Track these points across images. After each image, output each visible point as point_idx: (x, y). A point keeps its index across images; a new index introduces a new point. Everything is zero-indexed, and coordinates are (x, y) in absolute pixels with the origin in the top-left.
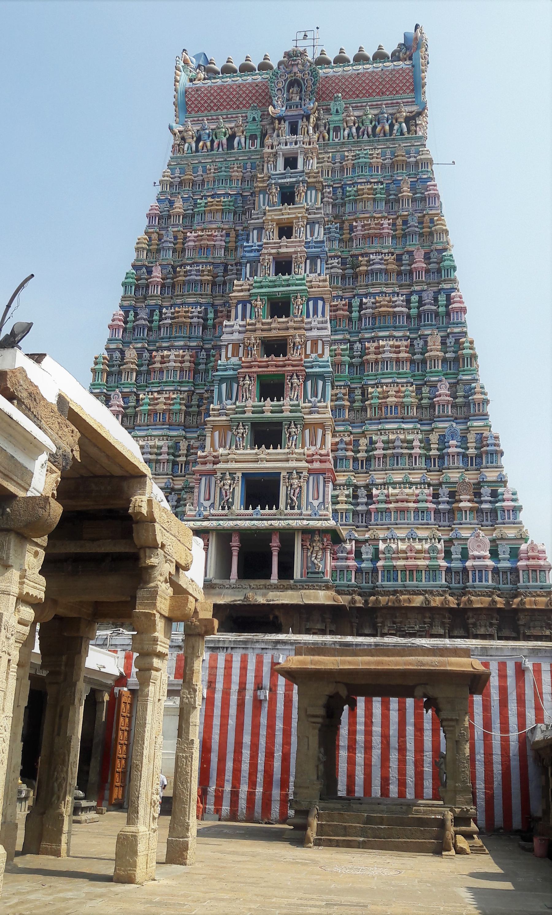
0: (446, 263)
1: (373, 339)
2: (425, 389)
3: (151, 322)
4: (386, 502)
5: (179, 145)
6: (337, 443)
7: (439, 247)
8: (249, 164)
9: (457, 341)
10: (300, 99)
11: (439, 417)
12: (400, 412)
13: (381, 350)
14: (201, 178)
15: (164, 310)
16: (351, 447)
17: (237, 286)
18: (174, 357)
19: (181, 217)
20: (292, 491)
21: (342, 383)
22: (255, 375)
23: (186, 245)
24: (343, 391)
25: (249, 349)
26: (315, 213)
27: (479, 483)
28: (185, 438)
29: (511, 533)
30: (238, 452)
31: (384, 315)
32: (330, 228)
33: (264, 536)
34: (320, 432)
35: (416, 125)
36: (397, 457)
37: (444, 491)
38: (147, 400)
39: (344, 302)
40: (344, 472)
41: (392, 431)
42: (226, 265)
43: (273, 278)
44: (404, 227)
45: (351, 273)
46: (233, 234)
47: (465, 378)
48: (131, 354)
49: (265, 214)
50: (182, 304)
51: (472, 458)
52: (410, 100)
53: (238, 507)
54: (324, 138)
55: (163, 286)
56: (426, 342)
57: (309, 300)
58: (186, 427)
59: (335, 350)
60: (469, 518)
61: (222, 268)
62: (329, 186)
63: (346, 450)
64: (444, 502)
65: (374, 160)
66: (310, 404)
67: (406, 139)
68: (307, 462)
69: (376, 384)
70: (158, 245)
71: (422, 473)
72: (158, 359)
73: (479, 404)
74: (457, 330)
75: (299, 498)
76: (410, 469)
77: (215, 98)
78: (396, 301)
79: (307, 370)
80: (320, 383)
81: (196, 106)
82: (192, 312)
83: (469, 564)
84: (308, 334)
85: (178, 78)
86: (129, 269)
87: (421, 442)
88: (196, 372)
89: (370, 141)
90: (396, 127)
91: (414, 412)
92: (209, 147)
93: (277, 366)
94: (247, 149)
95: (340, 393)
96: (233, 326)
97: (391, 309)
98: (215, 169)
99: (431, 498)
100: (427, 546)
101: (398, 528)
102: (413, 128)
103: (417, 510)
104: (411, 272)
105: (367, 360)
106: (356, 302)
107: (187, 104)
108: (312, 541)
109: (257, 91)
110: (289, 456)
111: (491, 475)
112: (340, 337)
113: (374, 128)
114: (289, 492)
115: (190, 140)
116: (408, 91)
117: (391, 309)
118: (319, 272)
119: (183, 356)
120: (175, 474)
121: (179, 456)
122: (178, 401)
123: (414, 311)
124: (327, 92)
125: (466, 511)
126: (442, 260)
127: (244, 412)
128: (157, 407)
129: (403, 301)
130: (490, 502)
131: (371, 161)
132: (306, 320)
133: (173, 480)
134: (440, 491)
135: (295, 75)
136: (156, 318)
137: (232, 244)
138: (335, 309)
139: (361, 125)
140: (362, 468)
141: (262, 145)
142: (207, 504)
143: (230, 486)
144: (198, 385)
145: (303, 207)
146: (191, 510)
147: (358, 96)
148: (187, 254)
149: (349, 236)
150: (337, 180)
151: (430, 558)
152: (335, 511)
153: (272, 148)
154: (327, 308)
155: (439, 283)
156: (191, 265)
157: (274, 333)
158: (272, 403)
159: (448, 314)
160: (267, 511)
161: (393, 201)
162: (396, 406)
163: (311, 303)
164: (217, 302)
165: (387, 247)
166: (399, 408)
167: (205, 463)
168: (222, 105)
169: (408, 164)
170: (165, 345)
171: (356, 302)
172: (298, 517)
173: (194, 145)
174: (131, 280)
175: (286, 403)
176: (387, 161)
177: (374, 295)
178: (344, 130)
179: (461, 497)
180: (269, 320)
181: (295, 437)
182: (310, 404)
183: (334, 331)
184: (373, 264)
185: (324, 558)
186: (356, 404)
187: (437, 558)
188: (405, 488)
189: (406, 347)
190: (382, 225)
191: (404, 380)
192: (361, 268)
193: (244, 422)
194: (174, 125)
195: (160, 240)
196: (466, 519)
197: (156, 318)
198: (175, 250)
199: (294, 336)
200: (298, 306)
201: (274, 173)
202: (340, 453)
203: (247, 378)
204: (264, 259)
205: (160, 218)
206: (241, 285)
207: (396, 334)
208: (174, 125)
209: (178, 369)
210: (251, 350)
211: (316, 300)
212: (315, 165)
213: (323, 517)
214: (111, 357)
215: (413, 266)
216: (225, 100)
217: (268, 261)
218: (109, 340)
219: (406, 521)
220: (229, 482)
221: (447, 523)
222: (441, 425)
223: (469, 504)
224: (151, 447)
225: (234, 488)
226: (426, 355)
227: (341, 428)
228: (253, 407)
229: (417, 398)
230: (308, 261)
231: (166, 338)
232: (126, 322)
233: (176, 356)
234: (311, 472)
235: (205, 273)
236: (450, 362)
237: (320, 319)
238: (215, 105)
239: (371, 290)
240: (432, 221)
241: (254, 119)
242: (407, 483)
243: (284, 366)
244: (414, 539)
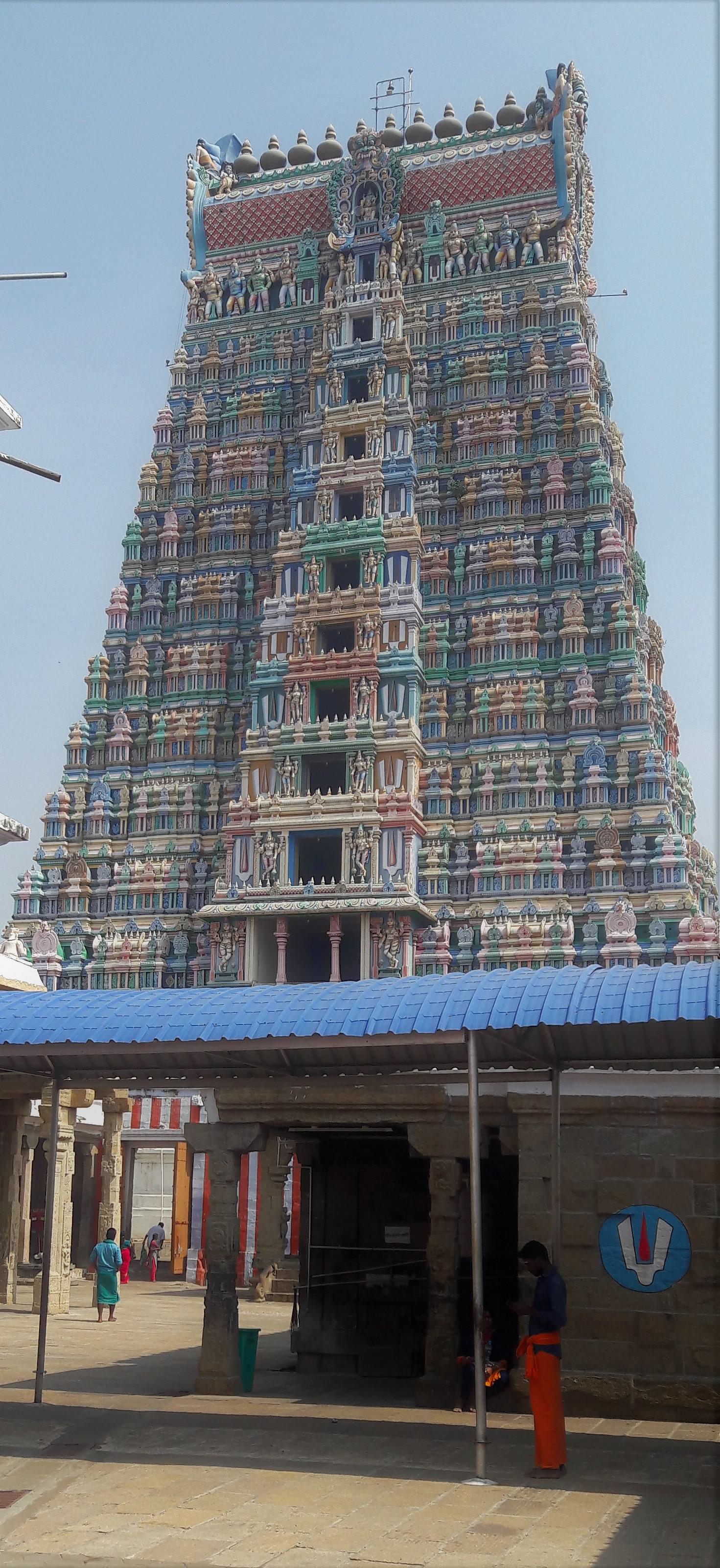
0: (595, 480)
1: (485, 610)
2: (559, 686)
3: (165, 600)
5: (197, 306)
6: (428, 777)
7: (587, 453)
8: (302, 331)
9: (608, 605)
10: (377, 216)
11: (577, 729)
12: (519, 725)
13: (494, 627)
14: (231, 359)
15: (183, 582)
16: (449, 781)
17: (283, 540)
18: (197, 653)
19: (204, 428)
20: (358, 855)
21: (437, 682)
22: (308, 683)
23: (211, 474)
24: (438, 695)
25: (300, 641)
26: (398, 413)
27: (631, 827)
28: (217, 776)
29: (670, 902)
30: (283, 800)
31: (500, 571)
32: (422, 432)
33: (322, 920)
35: (557, 245)
36: (513, 794)
37: (579, 842)
38: (162, 724)
39: (441, 553)
40: (438, 819)
41: (506, 754)
43: (334, 525)
44: (535, 422)
45: (454, 506)
46: (279, 450)
47: (617, 665)
48: (139, 654)
49: (323, 418)
50: (208, 570)
51: (623, 790)
52: (549, 199)
53: (284, 884)
54: (415, 275)
55: (180, 542)
58: (217, 761)
59: (427, 631)
60: (611, 883)
61: (265, 508)
62: (421, 360)
63: (441, 786)
65: (490, 312)
66: (385, 723)
67: (542, 269)
68: (379, 811)
69: (486, 681)
70: (171, 476)
71: (548, 817)
72: (176, 659)
73: (635, 706)
74: (608, 589)
75: (368, 865)
76: (531, 812)
77: (249, 221)
78: (519, 547)
79: (382, 671)
80: (401, 688)
81: (221, 237)
82: (222, 583)
83: (604, 950)
84: (382, 612)
85: (192, 192)
87: (548, 768)
88: (230, 675)
89: (485, 279)
90: (525, 251)
91: (541, 723)
92: (242, 306)
93: (338, 667)
94: (300, 306)
95: (433, 698)
96: (276, 606)
97: (508, 562)
98: (251, 344)
99: (560, 854)
100: (548, 927)
101: (510, 901)
102: (552, 249)
103: (537, 873)
104: (543, 496)
105: (473, 644)
107: (207, 234)
108: (384, 927)
109: (312, 205)
110: (353, 805)
111: (647, 816)
112: (435, 609)
113: (493, 253)
114: (353, 857)
115: (214, 296)
116: (546, 184)
118: (403, 509)
119: (211, 653)
120: (204, 831)
121: (209, 804)
122: (205, 722)
123: (545, 561)
124: (420, 197)
125: (607, 872)
126: (589, 475)
127: (292, 740)
128: (176, 734)
129: (529, 546)
130: (645, 856)
131: (485, 313)
132: (381, 590)
133: (202, 840)
134: (573, 843)
135: (367, 177)
136: (172, 593)
137: (278, 468)
138: (426, 565)
139: (471, 251)
140: (464, 811)
142: (244, 877)
143: (274, 852)
144: (233, 695)
145: (380, 405)
146: (221, 888)
147: (467, 199)
148: (215, 488)
149: (450, 443)
150: (436, 348)
151: (552, 944)
152: (421, 881)
153: (334, 307)
154: (415, 566)
155: (585, 513)
156: (219, 506)
157: (335, 615)
158: (330, 724)
159: (596, 562)
160: (323, 886)
161: (518, 379)
162: (514, 716)
163: (390, 561)
164: (259, 563)
165: (509, 458)
166: (519, 718)
167: (238, 819)
168: (259, 231)
169: (542, 312)
170: (185, 635)
172: (364, 893)
173: (219, 304)
174: (134, 537)
175: (351, 722)
176: (512, 310)
177: (486, 538)
178: (446, 261)
179: (601, 851)
180: (328, 595)
181: (364, 774)
182: (385, 723)
183: (427, 601)
184: (486, 488)
185: (401, 951)
186: (458, 714)
188: (522, 840)
189: (532, 620)
190: (501, 421)
191: (529, 673)
192: (467, 497)
193: (292, 754)
194: (188, 272)
195: (174, 466)
196: (607, 884)
197: (172, 593)
198: (195, 484)
199: (363, 618)
200: (371, 568)
201: (338, 348)
202: (432, 792)
203: (297, 688)
204: (321, 496)
205: (174, 432)
206: (290, 539)
207: (517, 600)
208: (188, 272)
209: (205, 673)
210: (303, 643)
211: (397, 556)
212: (401, 327)
213: (399, 893)
214: (112, 659)
215: (546, 488)
216: (263, 224)
217: (328, 499)
218: (108, 633)
219: (522, 889)
220: (272, 845)
221: (582, 890)
222: (578, 742)
223: (612, 862)
224: (170, 794)
225: (279, 854)
226: (562, 631)
227: (434, 753)
228: (305, 731)
229: (545, 702)
230: (387, 493)
231: (187, 625)
232: (130, 603)
233: (201, 653)
234: (383, 826)
235: (240, 518)
236: (598, 640)
237: (401, 587)
238: (249, 232)
239: (482, 531)
240: (577, 409)
241: (308, 253)
242: (525, 832)
243: (349, 666)
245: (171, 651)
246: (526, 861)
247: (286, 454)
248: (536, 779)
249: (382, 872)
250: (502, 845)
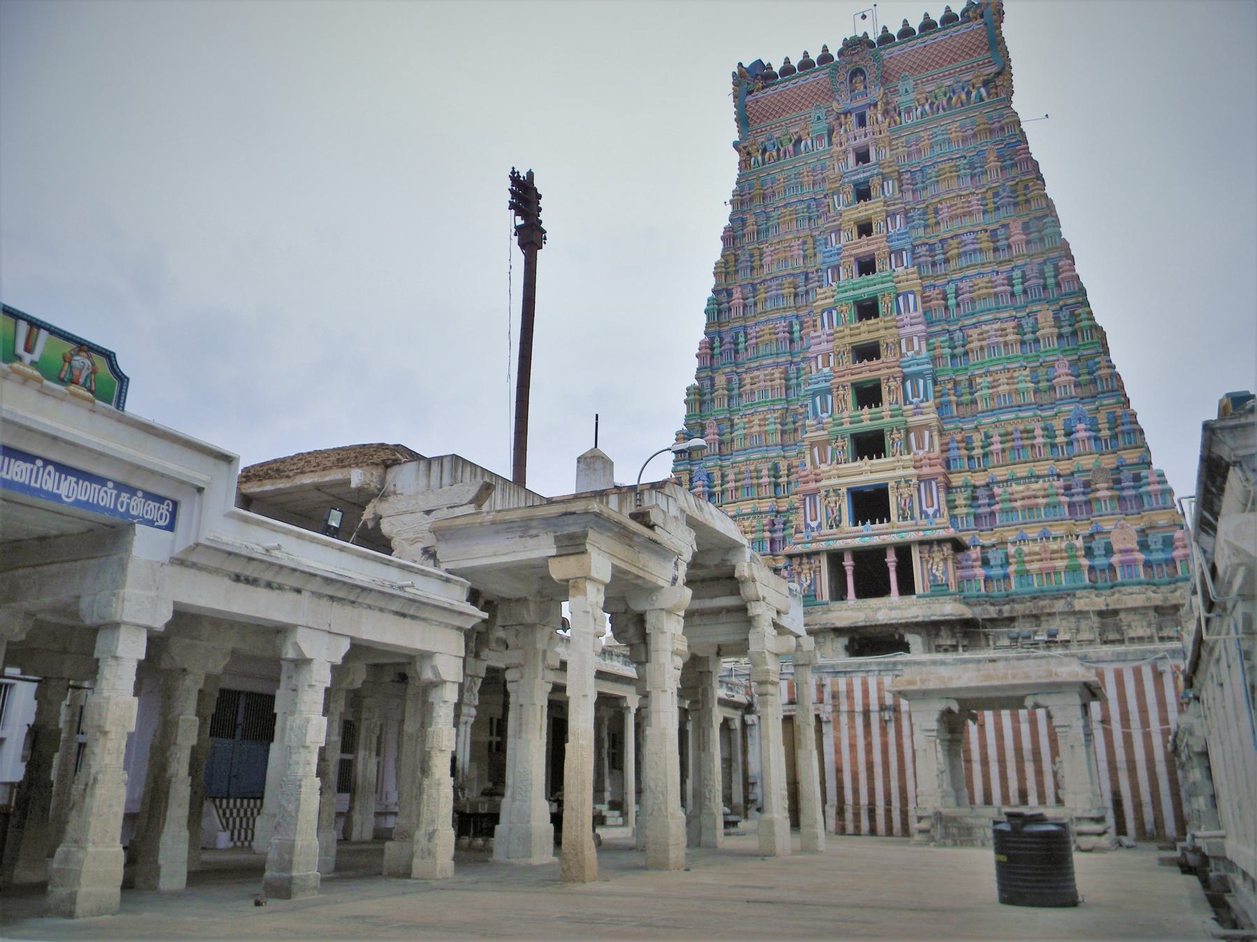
1: (975, 325)
4: (1011, 501)
9: (1072, 314)
27: (1117, 468)
34: (927, 433)
35: (996, 87)
42: (807, 274)
46: (810, 241)
48: (720, 380)
56: (1036, 319)
57: (898, 295)
64: (1078, 494)
75: (911, 509)
80: (921, 382)
84: (902, 331)
86: (710, 294)
87: (1043, 429)
88: (788, 388)
90: (974, 94)
91: (1031, 398)
97: (992, 291)
100: (1063, 545)
104: (1009, 247)
106: (950, 289)
112: (939, 328)
113: (950, 98)
117: (992, 291)
127: (842, 424)
136: (742, 339)
141: (830, 143)
154: (919, 298)
160: (878, 525)
163: (901, 299)
164: (801, 313)
171: (950, 289)
173: (760, 158)
175: (885, 407)
187: (1077, 557)
195: (736, 260)
221: (1085, 516)
222: (1064, 409)
241: (819, 118)
244: (1048, 538)
245: (744, 376)
246: (1035, 497)
248: (1035, 438)
249: (922, 512)
250: (1015, 488)
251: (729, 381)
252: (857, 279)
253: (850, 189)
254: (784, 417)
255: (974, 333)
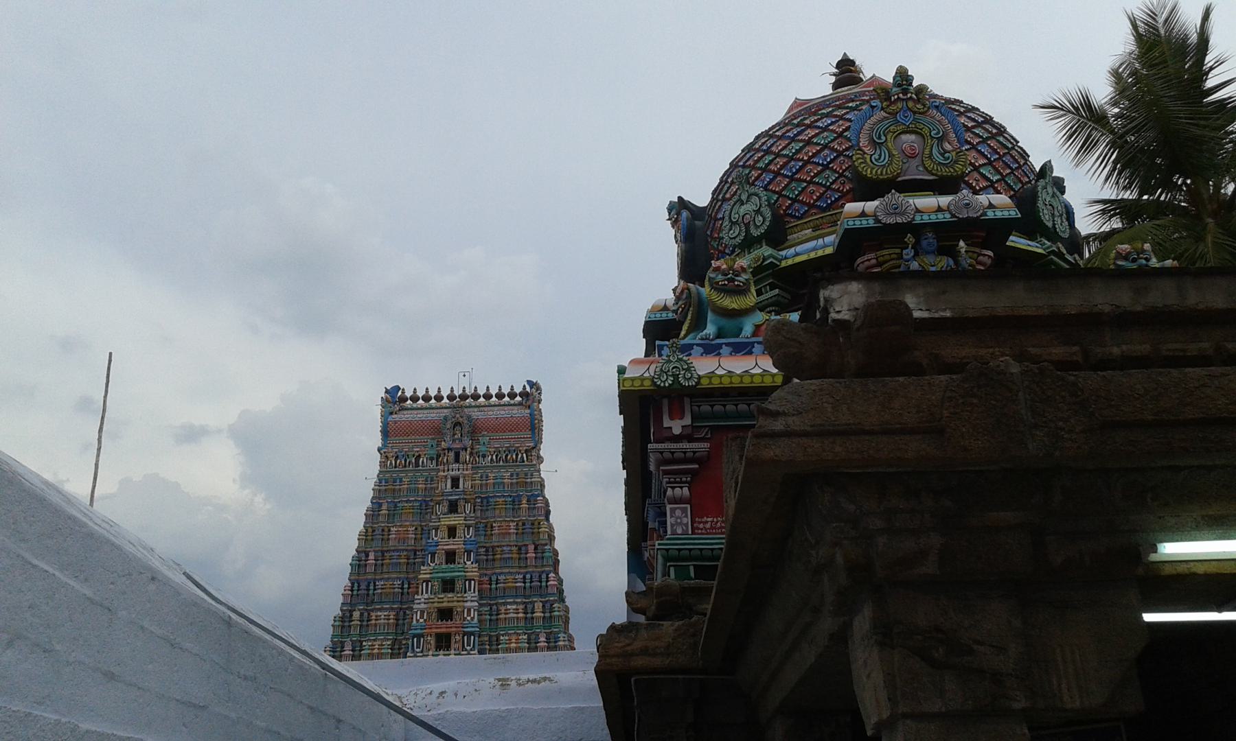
1: (505, 604)
48: (356, 614)
106: (494, 578)
123: (528, 585)
157: (445, 604)
200: (458, 586)
247: (423, 532)
251: (362, 615)
252: (444, 566)
253: (446, 504)
254: (393, 644)
255: (503, 608)
